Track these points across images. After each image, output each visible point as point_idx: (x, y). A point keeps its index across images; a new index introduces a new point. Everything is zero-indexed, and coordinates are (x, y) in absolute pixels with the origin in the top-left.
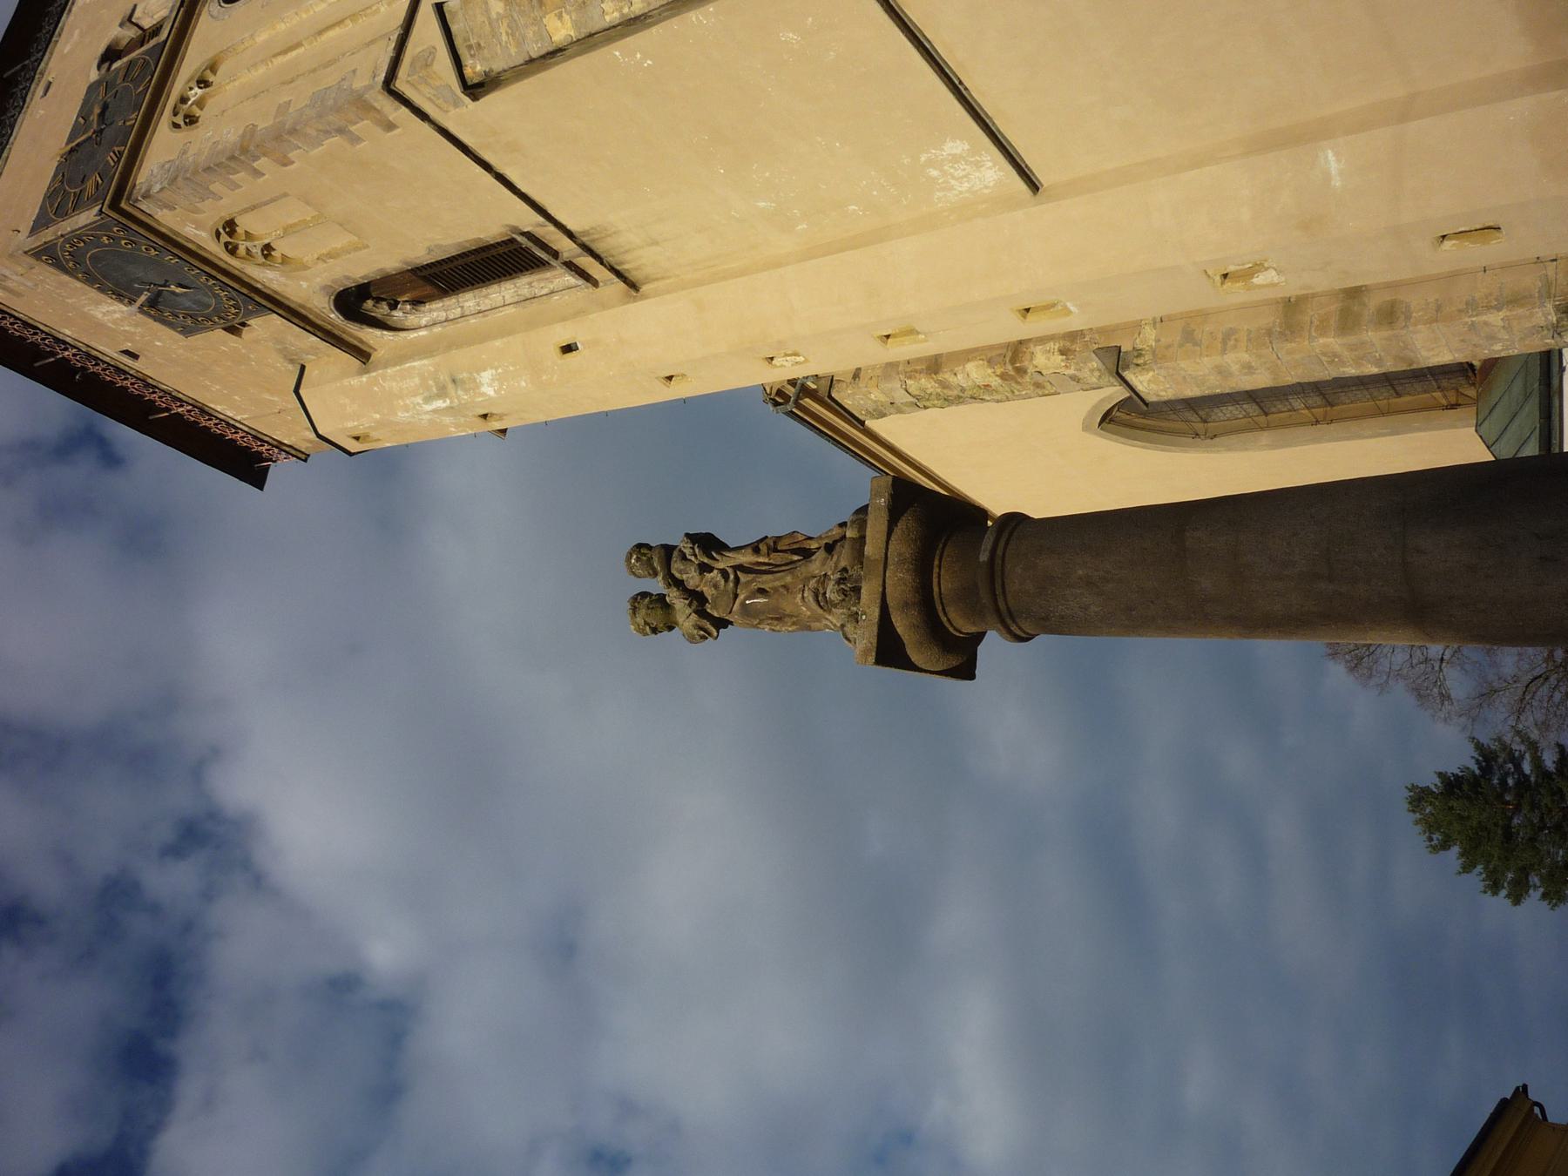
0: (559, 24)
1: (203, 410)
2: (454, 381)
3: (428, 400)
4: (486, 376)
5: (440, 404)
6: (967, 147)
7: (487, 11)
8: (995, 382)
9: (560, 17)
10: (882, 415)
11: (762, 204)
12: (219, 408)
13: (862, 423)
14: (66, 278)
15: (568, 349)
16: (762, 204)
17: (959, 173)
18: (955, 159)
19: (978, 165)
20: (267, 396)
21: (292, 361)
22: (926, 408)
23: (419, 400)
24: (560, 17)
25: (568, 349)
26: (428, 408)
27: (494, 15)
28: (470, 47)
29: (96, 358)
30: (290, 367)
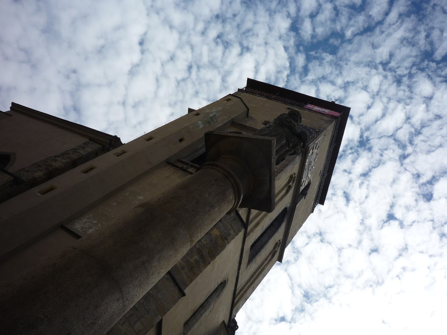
0: (216, 233)
1: (268, 97)
2: (209, 123)
3: (215, 115)
4: (201, 126)
5: (211, 115)
6: (88, 233)
7: (234, 230)
8: (54, 164)
9: (216, 235)
10: (84, 143)
11: (141, 197)
12: (265, 99)
13: (90, 139)
14: (311, 126)
15: (181, 140)
16: (141, 197)
17: (87, 224)
18: (90, 228)
19: (82, 228)
20: (254, 105)
21: (251, 117)
22: (72, 149)
23: (217, 115)
24: (216, 235)
25: (181, 140)
26: (214, 113)
27: (232, 230)
28: (236, 219)
29: (298, 106)
30: (251, 115)
